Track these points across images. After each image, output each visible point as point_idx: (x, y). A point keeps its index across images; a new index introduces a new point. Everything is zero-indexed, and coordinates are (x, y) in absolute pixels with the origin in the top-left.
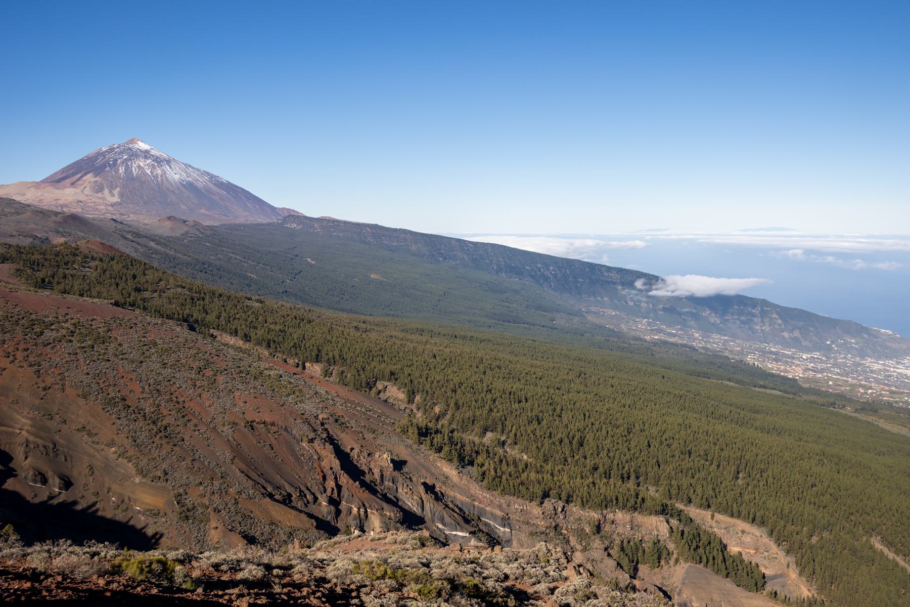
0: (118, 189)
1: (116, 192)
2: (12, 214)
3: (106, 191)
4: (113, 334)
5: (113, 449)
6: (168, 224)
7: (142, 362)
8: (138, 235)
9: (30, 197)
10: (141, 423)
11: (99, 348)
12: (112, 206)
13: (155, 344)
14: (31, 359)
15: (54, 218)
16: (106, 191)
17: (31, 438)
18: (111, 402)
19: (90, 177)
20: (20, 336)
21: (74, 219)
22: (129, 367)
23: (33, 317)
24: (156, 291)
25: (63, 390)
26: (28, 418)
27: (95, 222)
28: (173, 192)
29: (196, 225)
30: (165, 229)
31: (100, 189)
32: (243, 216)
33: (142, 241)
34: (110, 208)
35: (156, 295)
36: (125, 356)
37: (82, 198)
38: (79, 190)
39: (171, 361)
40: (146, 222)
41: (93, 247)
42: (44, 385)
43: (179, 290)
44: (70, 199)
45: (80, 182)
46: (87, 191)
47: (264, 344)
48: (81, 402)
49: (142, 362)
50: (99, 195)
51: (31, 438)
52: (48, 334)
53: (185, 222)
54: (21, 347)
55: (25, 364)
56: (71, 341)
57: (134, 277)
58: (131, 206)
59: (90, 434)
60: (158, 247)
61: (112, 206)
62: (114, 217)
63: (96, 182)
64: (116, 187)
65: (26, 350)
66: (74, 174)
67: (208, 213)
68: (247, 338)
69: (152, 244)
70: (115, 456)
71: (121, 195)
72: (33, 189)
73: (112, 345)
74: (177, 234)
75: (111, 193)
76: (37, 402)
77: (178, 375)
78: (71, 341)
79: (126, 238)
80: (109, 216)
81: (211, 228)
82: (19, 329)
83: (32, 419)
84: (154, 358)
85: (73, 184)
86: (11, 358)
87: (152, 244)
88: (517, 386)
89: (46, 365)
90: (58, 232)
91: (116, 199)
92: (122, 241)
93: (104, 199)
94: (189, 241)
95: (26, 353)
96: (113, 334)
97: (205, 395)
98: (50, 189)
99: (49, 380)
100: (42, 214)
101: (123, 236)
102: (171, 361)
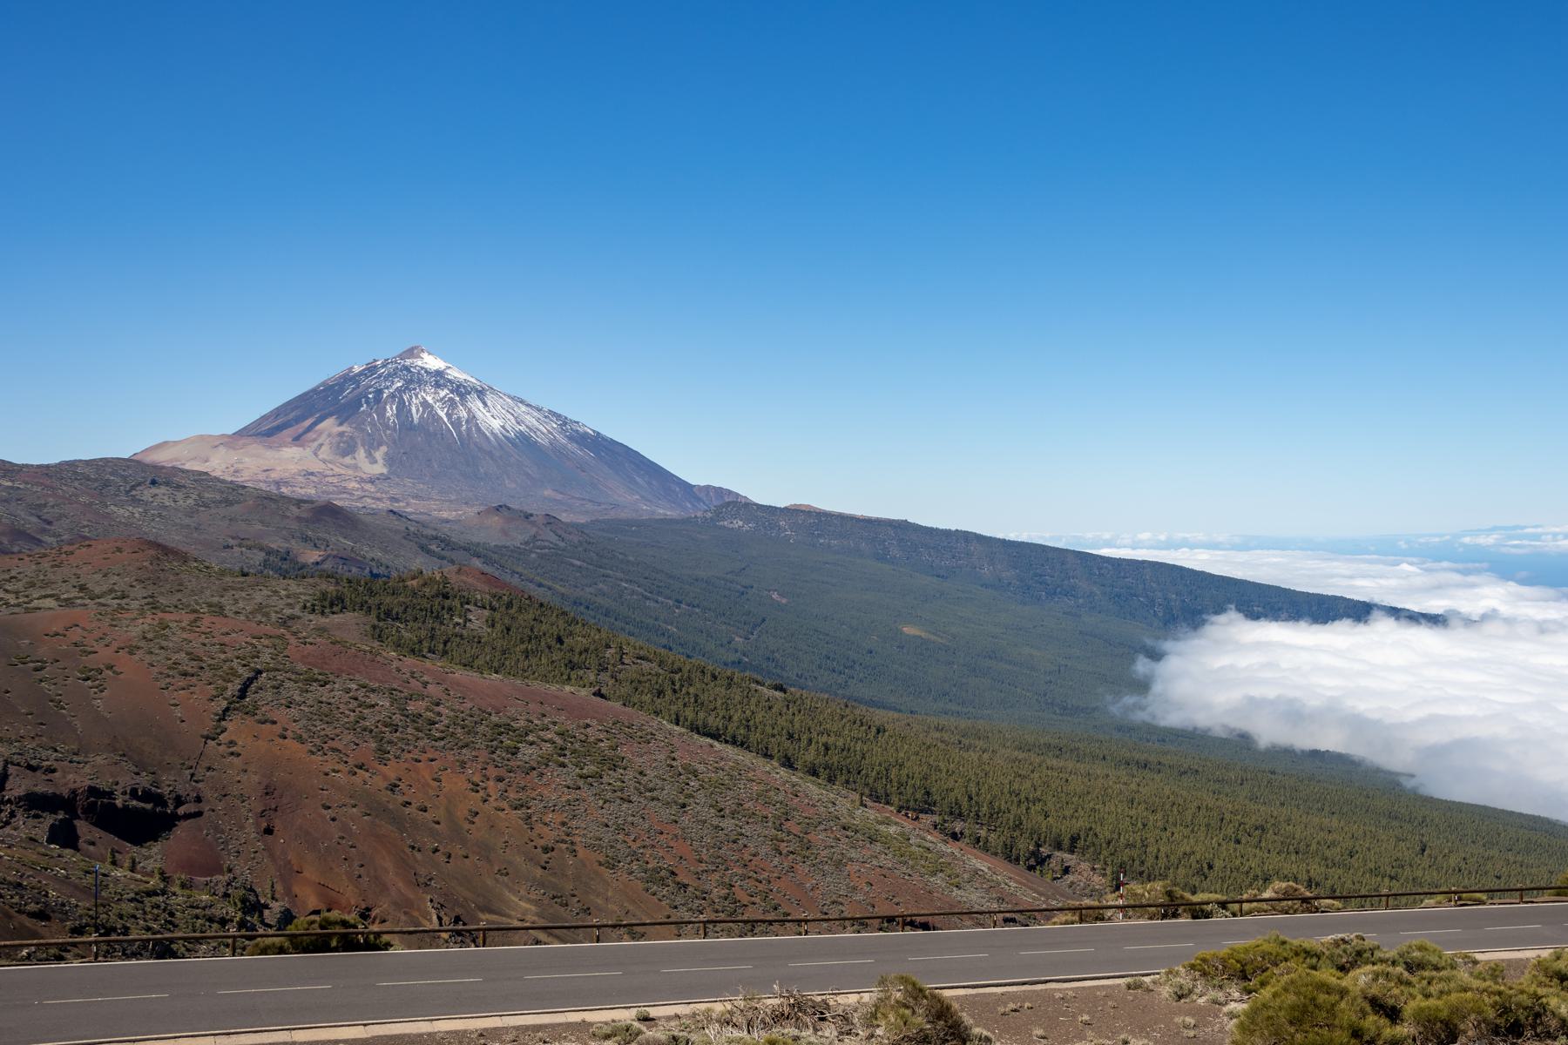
0: (384, 449)
3: (361, 453)
6: (495, 521)
7: (684, 806)
8: (446, 543)
9: (218, 465)
11: (609, 777)
12: (372, 481)
13: (695, 774)
14: (512, 795)
15: (294, 509)
16: (361, 453)
18: (656, 877)
19: (329, 425)
20: (484, 755)
21: (328, 514)
22: (667, 813)
23: (494, 719)
26: (529, 901)
27: (368, 519)
28: (490, 454)
29: (550, 520)
30: (491, 533)
31: (346, 448)
32: (631, 502)
34: (368, 486)
36: (655, 794)
37: (317, 467)
38: (308, 452)
39: (729, 805)
40: (445, 515)
41: (470, 580)
42: (542, 842)
44: (293, 468)
45: (311, 435)
46: (325, 453)
47: (824, 774)
48: (607, 873)
49: (684, 806)
50: (348, 460)
52: (528, 753)
53: (528, 516)
54: (492, 772)
55: (504, 804)
56: (563, 765)
57: (560, 640)
58: (408, 482)
61: (372, 481)
62: (396, 506)
63: (341, 434)
64: (380, 445)
65: (500, 779)
66: (298, 420)
67: (559, 497)
68: (788, 763)
71: (389, 460)
72: (221, 448)
73: (630, 774)
74: (518, 538)
76: (539, 872)
77: (747, 830)
78: (563, 765)
79: (429, 552)
80: (384, 505)
81: (579, 528)
82: (481, 743)
83: (536, 903)
84: (700, 796)
85: (297, 439)
86: (482, 793)
88: (1316, 870)
89: (536, 806)
90: (306, 539)
91: (380, 469)
93: (356, 467)
94: (542, 556)
95: (501, 785)
97: (803, 869)
98: (256, 448)
99: (550, 836)
101: (422, 548)
102: (729, 805)
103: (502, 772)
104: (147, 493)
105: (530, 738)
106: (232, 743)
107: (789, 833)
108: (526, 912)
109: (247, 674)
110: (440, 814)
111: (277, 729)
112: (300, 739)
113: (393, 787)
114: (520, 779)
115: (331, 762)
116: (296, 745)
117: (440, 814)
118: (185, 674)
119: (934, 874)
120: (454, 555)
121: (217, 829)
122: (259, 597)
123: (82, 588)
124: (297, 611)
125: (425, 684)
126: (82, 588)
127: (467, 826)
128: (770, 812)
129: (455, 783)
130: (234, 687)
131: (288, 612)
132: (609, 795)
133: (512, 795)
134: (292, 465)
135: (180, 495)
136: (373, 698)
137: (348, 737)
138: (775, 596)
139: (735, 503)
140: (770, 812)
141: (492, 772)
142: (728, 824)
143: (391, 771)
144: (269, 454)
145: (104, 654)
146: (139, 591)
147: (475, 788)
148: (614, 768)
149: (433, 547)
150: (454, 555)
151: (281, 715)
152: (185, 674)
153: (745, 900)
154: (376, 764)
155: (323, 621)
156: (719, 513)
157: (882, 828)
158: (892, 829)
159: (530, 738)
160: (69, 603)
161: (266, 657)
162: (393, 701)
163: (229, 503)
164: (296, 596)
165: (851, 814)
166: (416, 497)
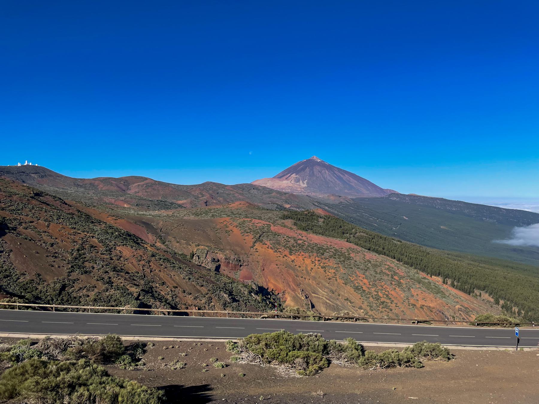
1: (305, 182)
2: (267, 194)
4: (351, 255)
5: (362, 311)
9: (269, 185)
10: (371, 299)
17: (328, 301)
19: (294, 175)
20: (315, 254)
23: (319, 246)
24: (351, 234)
25: (336, 280)
31: (299, 181)
32: (366, 193)
33: (322, 206)
35: (352, 236)
37: (291, 185)
38: (289, 182)
42: (329, 277)
43: (362, 234)
44: (285, 185)
50: (298, 183)
51: (328, 301)
52: (326, 254)
55: (320, 267)
59: (350, 302)
60: (329, 209)
65: (319, 261)
66: (287, 174)
69: (326, 208)
70: (363, 314)
71: (308, 183)
73: (352, 261)
74: (337, 202)
75: (303, 182)
77: (383, 278)
79: (315, 205)
80: (307, 194)
87: (326, 208)
90: (286, 202)
91: (305, 185)
92: (313, 206)
93: (300, 185)
96: (351, 255)
100: (278, 192)
103: (319, 259)
104: (252, 191)
105: (327, 251)
106: (257, 249)
107: (395, 279)
108: (323, 295)
109: (261, 233)
110: (304, 268)
111: (267, 246)
112: (271, 248)
113: (293, 261)
114: (323, 261)
115: (279, 254)
116: (270, 250)
117: (304, 268)
118: (247, 232)
119: (437, 294)
120: (321, 206)
121: (252, 269)
122: (270, 215)
123: (232, 213)
124: (278, 218)
125: (302, 237)
126: (232, 213)
127: (310, 272)
128: (390, 273)
129: (308, 261)
130: (258, 236)
131: (276, 219)
132: (346, 266)
133: (322, 264)
134: (285, 185)
135: (259, 192)
136: (290, 240)
137: (283, 248)
138: (405, 218)
139: (394, 194)
140: (390, 273)
141: (317, 259)
142: (378, 276)
143: (292, 257)
144: (281, 182)
145: (231, 227)
146: (244, 213)
147: (313, 262)
148: (349, 259)
149: (316, 204)
150: (321, 206)
151: (268, 243)
152: (247, 232)
153: (381, 296)
154: (289, 255)
155: (283, 221)
156: (390, 195)
157: (423, 280)
158: (426, 281)
159: (327, 251)
160: (229, 216)
161: (266, 229)
162: (294, 240)
163: (269, 193)
164: (278, 215)
165: (414, 276)
166: (314, 192)
